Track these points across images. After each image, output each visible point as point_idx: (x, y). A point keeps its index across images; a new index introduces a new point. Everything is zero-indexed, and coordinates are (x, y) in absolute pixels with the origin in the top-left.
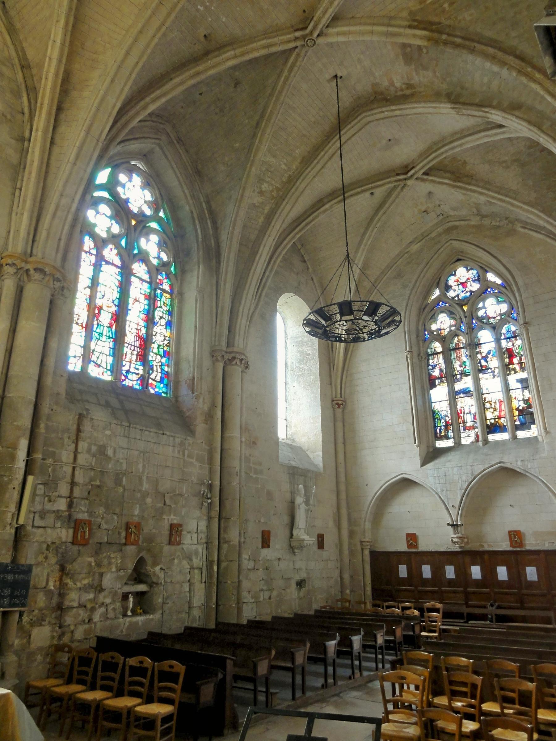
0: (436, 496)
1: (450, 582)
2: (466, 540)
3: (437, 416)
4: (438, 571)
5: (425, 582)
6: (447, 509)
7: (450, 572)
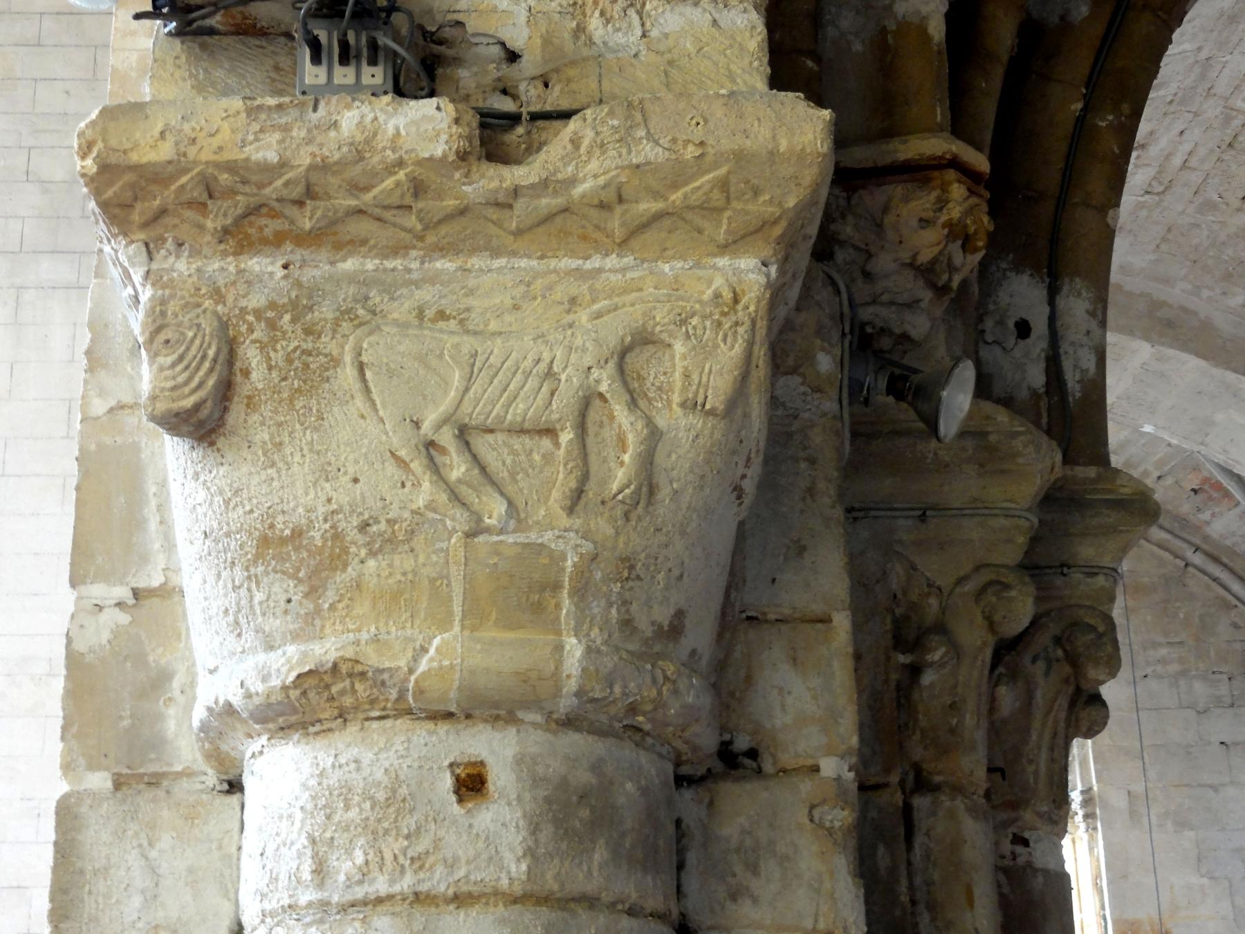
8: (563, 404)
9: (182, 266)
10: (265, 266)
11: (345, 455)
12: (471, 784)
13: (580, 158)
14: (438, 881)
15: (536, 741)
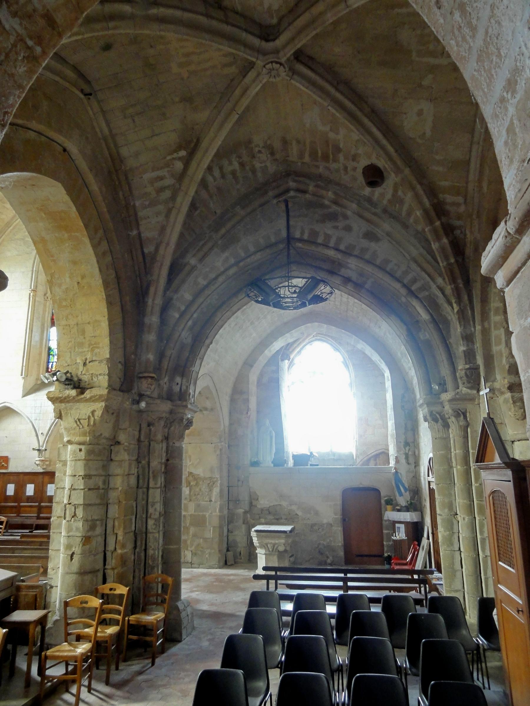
0: (30, 424)
1: (29, 499)
2: (47, 463)
3: (52, 353)
4: (20, 489)
5: (7, 498)
6: (37, 436)
7: (30, 490)
8: (87, 417)
9: (57, 405)
10: (63, 404)
11: (68, 422)
12: (80, 450)
13: (88, 394)
14: (77, 458)
15: (86, 446)
